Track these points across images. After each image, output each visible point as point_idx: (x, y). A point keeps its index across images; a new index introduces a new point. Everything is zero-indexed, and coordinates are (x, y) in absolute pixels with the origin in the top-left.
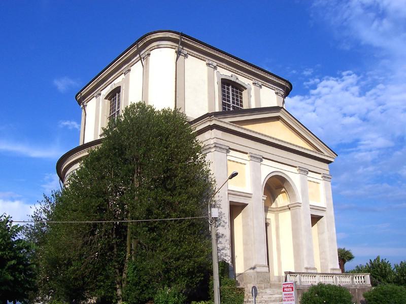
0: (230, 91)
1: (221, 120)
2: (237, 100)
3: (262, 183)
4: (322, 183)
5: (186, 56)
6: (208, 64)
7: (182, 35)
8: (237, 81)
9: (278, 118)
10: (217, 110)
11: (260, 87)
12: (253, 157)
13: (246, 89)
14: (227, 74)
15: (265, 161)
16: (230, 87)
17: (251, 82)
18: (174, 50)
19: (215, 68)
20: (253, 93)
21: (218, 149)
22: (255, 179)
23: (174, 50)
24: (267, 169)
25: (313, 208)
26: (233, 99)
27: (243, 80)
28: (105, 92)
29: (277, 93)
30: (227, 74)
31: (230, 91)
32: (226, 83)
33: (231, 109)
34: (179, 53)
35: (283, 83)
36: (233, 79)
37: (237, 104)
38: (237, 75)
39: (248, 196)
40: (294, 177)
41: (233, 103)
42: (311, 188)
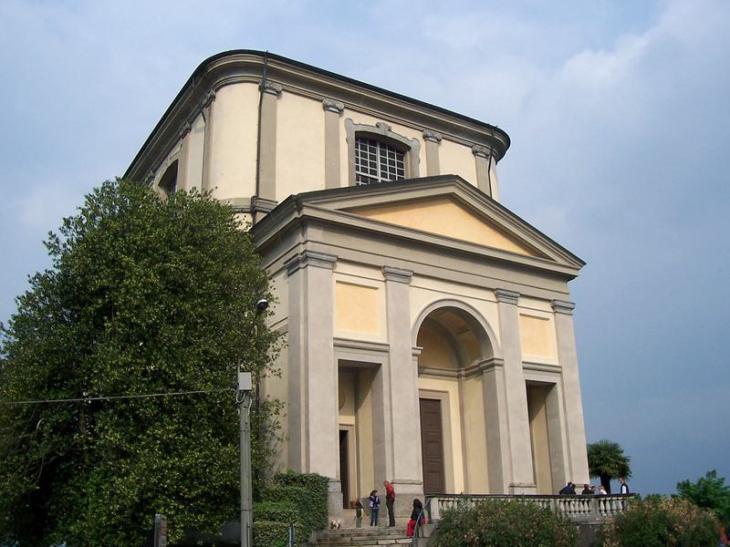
0: (379, 156)
3: (412, 322)
4: (551, 316)
5: (278, 94)
6: (326, 107)
8: (390, 135)
12: (388, 273)
13: (409, 148)
14: (368, 122)
15: (416, 281)
16: (378, 149)
17: (419, 135)
18: (257, 86)
19: (340, 112)
20: (422, 155)
21: (313, 262)
22: (394, 318)
23: (257, 86)
24: (423, 298)
26: (383, 168)
27: (401, 132)
28: (159, 175)
30: (368, 122)
31: (379, 156)
32: (364, 139)
34: (262, 90)
38: (389, 124)
39: (382, 349)
40: (486, 309)
42: (526, 330)
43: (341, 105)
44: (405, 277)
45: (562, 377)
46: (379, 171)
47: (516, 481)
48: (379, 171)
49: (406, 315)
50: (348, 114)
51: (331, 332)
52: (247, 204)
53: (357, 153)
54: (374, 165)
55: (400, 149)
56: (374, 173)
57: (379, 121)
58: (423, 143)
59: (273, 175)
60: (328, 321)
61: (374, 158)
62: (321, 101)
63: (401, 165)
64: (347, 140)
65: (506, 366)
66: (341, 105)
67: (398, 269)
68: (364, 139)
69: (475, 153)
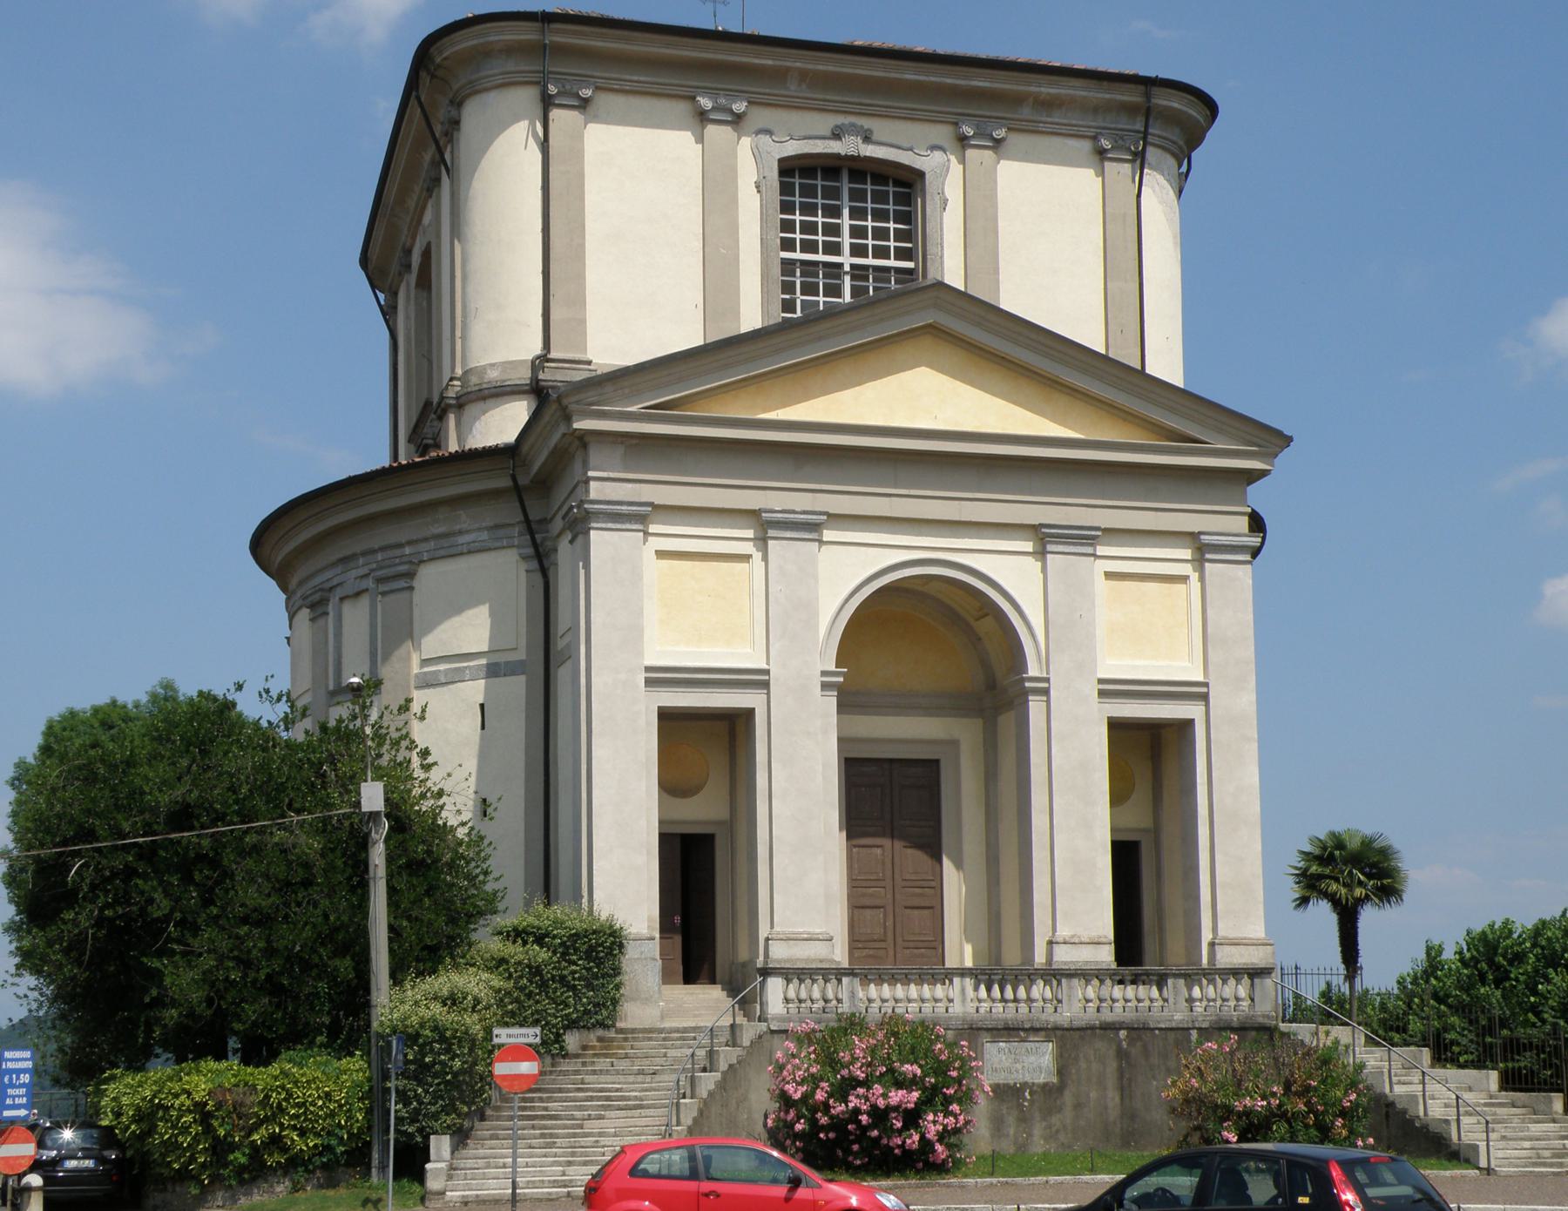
25: (1110, 690)
40: (1011, 572)
43: (739, 106)
44: (809, 527)
45: (1207, 706)
46: (846, 241)
47: (1063, 932)
48: (846, 241)
49: (809, 608)
51: (640, 654)
52: (523, 376)
53: (787, 207)
56: (834, 249)
57: (841, 120)
59: (579, 301)
60: (634, 635)
64: (757, 187)
65: (1053, 693)
66: (739, 106)
67: (794, 512)
68: (802, 178)
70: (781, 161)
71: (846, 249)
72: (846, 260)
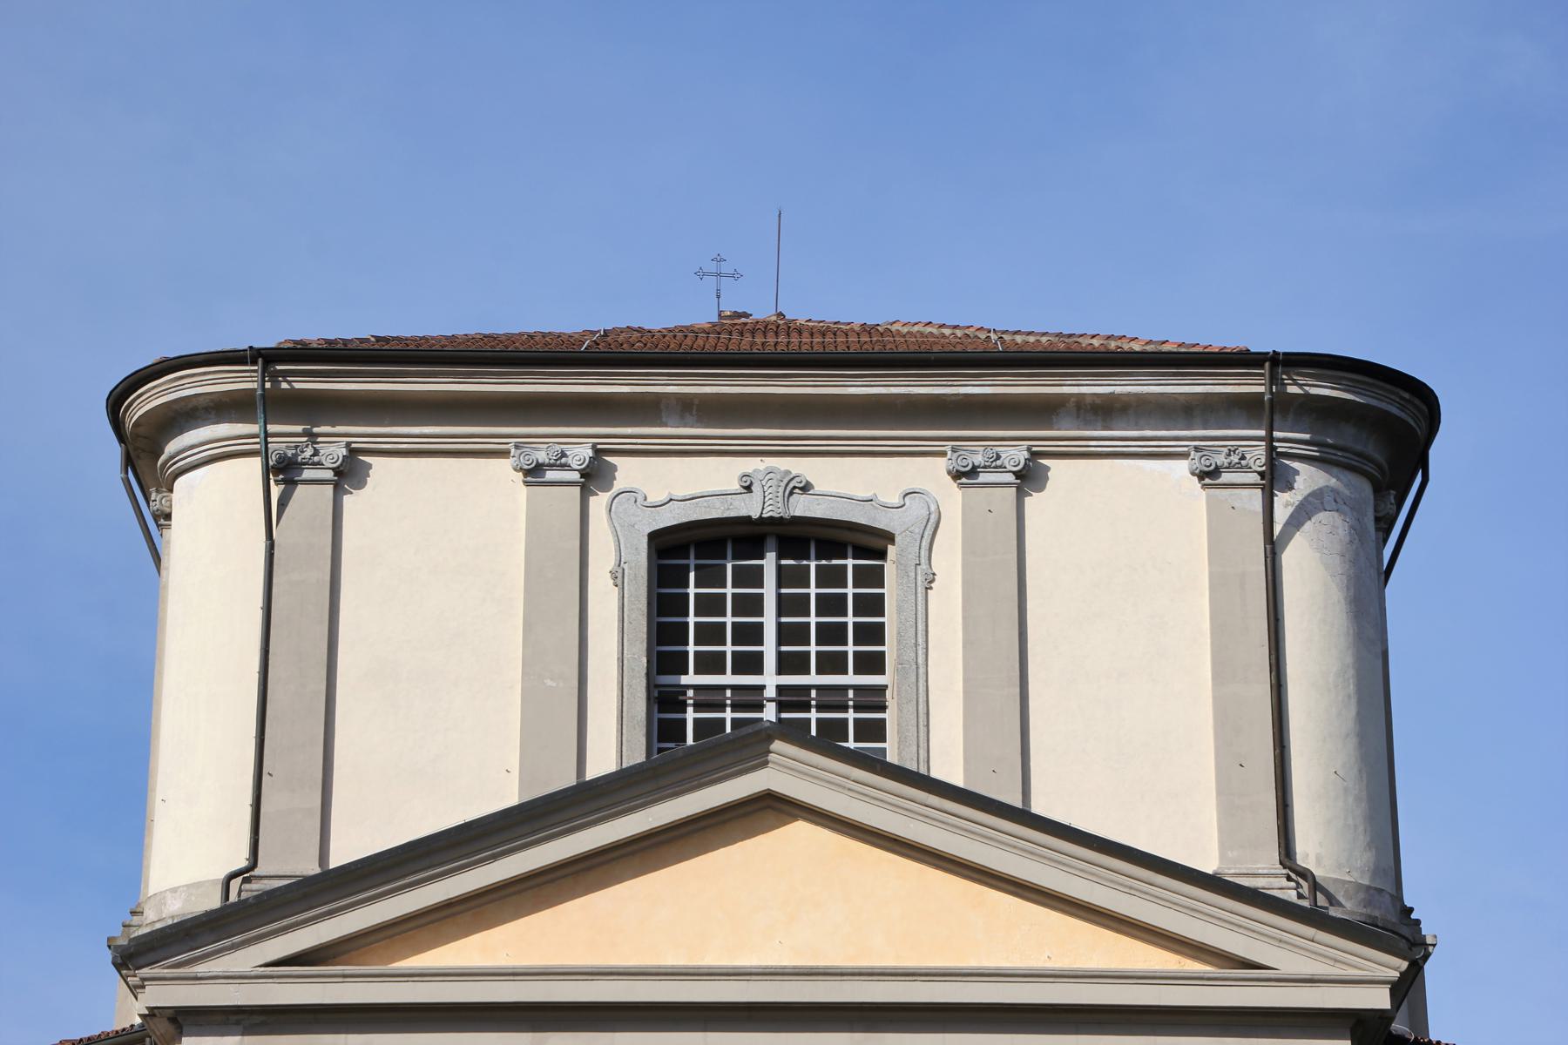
0: (769, 591)
1: (201, 969)
2: (830, 634)
5: (349, 474)
7: (267, 358)
8: (802, 507)
9: (772, 809)
10: (602, 761)
11: (1029, 478)
13: (889, 537)
16: (769, 563)
17: (927, 475)
19: (594, 476)
20: (948, 559)
23: (256, 464)
26: (784, 634)
29: (1215, 473)
31: (769, 591)
32: (680, 552)
33: (770, 713)
34: (284, 471)
35: (1254, 386)
36: (751, 507)
37: (831, 664)
41: (788, 664)
46: (769, 649)
48: (769, 649)
50: (628, 471)
54: (752, 634)
55: (857, 544)
56: (751, 664)
58: (951, 499)
61: (752, 605)
62: (504, 454)
63: (873, 605)
69: (1208, 475)
70: (654, 537)
71: (770, 661)
72: (770, 680)
